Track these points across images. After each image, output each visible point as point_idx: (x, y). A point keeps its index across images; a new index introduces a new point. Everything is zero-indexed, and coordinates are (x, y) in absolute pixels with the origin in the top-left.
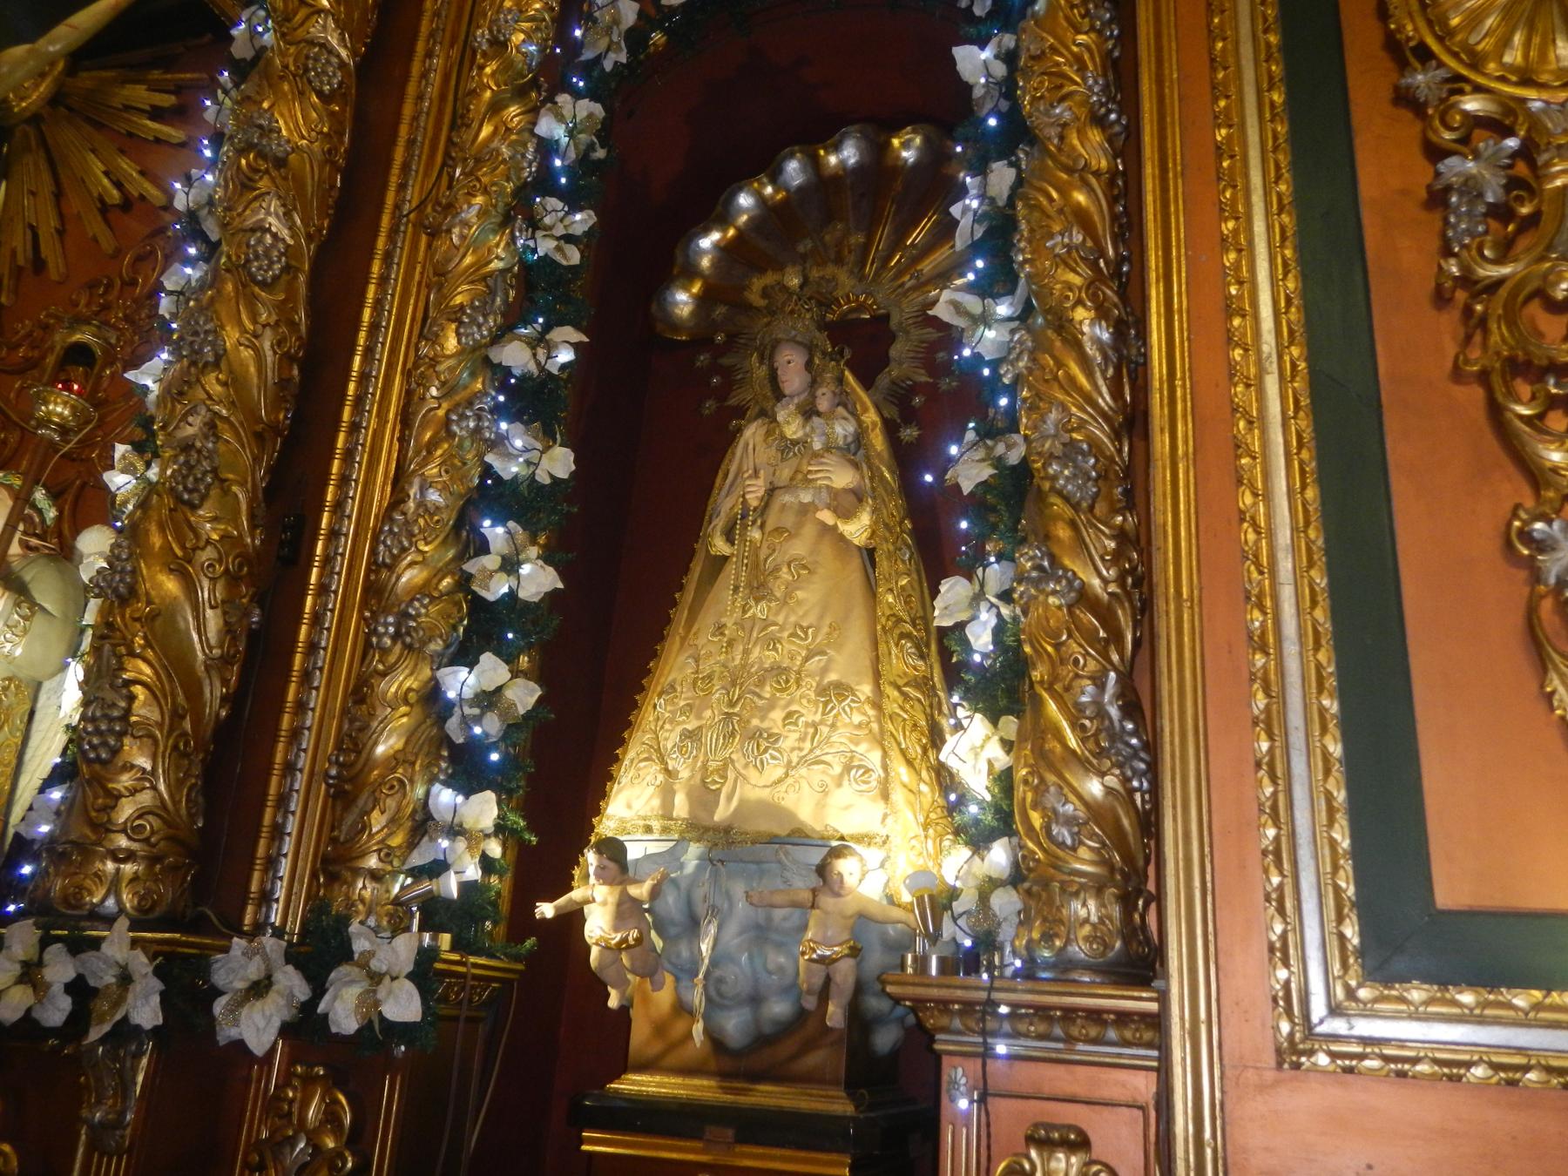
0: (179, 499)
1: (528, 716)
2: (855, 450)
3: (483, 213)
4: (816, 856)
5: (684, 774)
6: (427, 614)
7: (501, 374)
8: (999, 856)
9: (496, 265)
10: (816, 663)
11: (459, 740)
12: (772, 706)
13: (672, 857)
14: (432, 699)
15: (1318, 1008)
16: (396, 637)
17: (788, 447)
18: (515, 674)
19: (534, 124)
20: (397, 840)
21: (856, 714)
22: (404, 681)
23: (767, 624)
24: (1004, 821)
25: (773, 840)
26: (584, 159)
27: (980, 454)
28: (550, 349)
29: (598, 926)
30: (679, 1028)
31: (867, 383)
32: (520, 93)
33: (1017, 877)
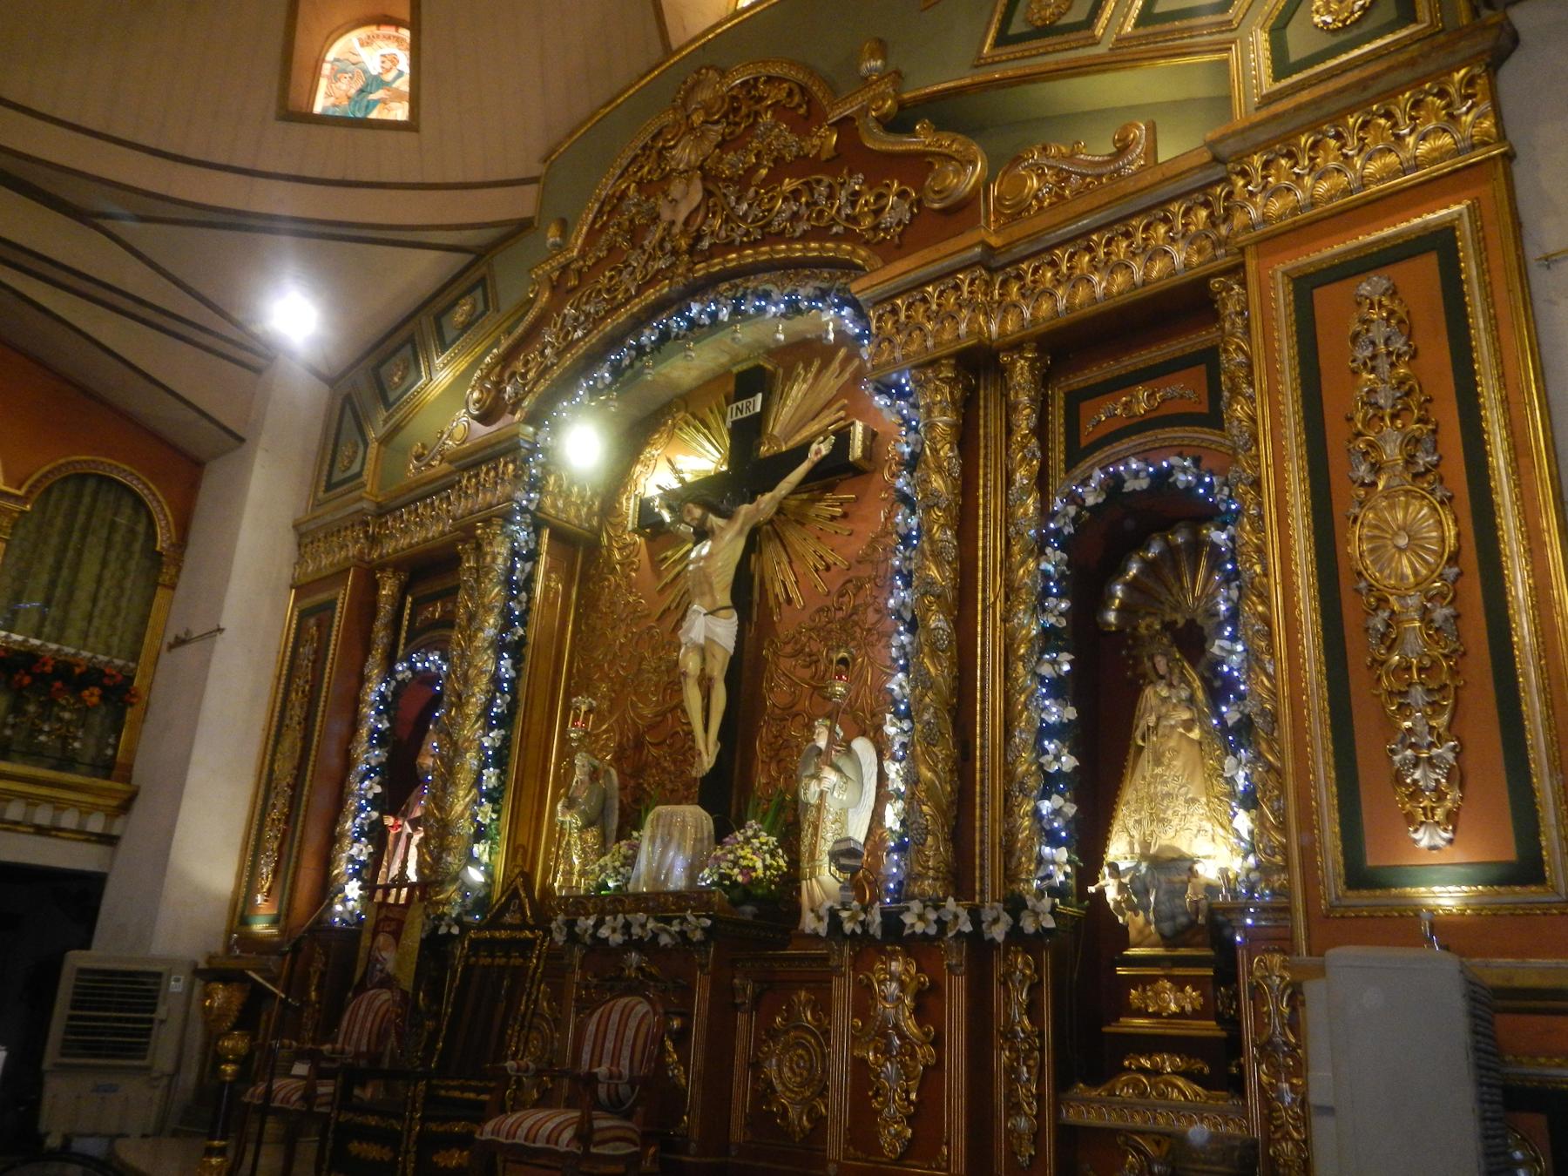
0: (928, 743)
1: (1074, 817)
2: (1191, 701)
3: (1025, 613)
4: (1188, 864)
5: (1137, 837)
6: (1031, 782)
7: (1042, 679)
9: (1034, 632)
10: (1183, 790)
11: (1048, 827)
12: (1168, 807)
13: (1136, 868)
14: (1036, 811)
16: (1020, 791)
17: (1165, 700)
18: (1066, 801)
19: (1038, 565)
20: (1032, 867)
21: (1200, 809)
22: (1027, 807)
23: (1162, 776)
24: (1253, 849)
25: (1173, 860)
26: (1063, 576)
27: (1235, 708)
28: (1059, 664)
29: (1112, 894)
30: (1147, 932)
31: (1194, 666)
32: (1031, 553)
33: (1259, 866)
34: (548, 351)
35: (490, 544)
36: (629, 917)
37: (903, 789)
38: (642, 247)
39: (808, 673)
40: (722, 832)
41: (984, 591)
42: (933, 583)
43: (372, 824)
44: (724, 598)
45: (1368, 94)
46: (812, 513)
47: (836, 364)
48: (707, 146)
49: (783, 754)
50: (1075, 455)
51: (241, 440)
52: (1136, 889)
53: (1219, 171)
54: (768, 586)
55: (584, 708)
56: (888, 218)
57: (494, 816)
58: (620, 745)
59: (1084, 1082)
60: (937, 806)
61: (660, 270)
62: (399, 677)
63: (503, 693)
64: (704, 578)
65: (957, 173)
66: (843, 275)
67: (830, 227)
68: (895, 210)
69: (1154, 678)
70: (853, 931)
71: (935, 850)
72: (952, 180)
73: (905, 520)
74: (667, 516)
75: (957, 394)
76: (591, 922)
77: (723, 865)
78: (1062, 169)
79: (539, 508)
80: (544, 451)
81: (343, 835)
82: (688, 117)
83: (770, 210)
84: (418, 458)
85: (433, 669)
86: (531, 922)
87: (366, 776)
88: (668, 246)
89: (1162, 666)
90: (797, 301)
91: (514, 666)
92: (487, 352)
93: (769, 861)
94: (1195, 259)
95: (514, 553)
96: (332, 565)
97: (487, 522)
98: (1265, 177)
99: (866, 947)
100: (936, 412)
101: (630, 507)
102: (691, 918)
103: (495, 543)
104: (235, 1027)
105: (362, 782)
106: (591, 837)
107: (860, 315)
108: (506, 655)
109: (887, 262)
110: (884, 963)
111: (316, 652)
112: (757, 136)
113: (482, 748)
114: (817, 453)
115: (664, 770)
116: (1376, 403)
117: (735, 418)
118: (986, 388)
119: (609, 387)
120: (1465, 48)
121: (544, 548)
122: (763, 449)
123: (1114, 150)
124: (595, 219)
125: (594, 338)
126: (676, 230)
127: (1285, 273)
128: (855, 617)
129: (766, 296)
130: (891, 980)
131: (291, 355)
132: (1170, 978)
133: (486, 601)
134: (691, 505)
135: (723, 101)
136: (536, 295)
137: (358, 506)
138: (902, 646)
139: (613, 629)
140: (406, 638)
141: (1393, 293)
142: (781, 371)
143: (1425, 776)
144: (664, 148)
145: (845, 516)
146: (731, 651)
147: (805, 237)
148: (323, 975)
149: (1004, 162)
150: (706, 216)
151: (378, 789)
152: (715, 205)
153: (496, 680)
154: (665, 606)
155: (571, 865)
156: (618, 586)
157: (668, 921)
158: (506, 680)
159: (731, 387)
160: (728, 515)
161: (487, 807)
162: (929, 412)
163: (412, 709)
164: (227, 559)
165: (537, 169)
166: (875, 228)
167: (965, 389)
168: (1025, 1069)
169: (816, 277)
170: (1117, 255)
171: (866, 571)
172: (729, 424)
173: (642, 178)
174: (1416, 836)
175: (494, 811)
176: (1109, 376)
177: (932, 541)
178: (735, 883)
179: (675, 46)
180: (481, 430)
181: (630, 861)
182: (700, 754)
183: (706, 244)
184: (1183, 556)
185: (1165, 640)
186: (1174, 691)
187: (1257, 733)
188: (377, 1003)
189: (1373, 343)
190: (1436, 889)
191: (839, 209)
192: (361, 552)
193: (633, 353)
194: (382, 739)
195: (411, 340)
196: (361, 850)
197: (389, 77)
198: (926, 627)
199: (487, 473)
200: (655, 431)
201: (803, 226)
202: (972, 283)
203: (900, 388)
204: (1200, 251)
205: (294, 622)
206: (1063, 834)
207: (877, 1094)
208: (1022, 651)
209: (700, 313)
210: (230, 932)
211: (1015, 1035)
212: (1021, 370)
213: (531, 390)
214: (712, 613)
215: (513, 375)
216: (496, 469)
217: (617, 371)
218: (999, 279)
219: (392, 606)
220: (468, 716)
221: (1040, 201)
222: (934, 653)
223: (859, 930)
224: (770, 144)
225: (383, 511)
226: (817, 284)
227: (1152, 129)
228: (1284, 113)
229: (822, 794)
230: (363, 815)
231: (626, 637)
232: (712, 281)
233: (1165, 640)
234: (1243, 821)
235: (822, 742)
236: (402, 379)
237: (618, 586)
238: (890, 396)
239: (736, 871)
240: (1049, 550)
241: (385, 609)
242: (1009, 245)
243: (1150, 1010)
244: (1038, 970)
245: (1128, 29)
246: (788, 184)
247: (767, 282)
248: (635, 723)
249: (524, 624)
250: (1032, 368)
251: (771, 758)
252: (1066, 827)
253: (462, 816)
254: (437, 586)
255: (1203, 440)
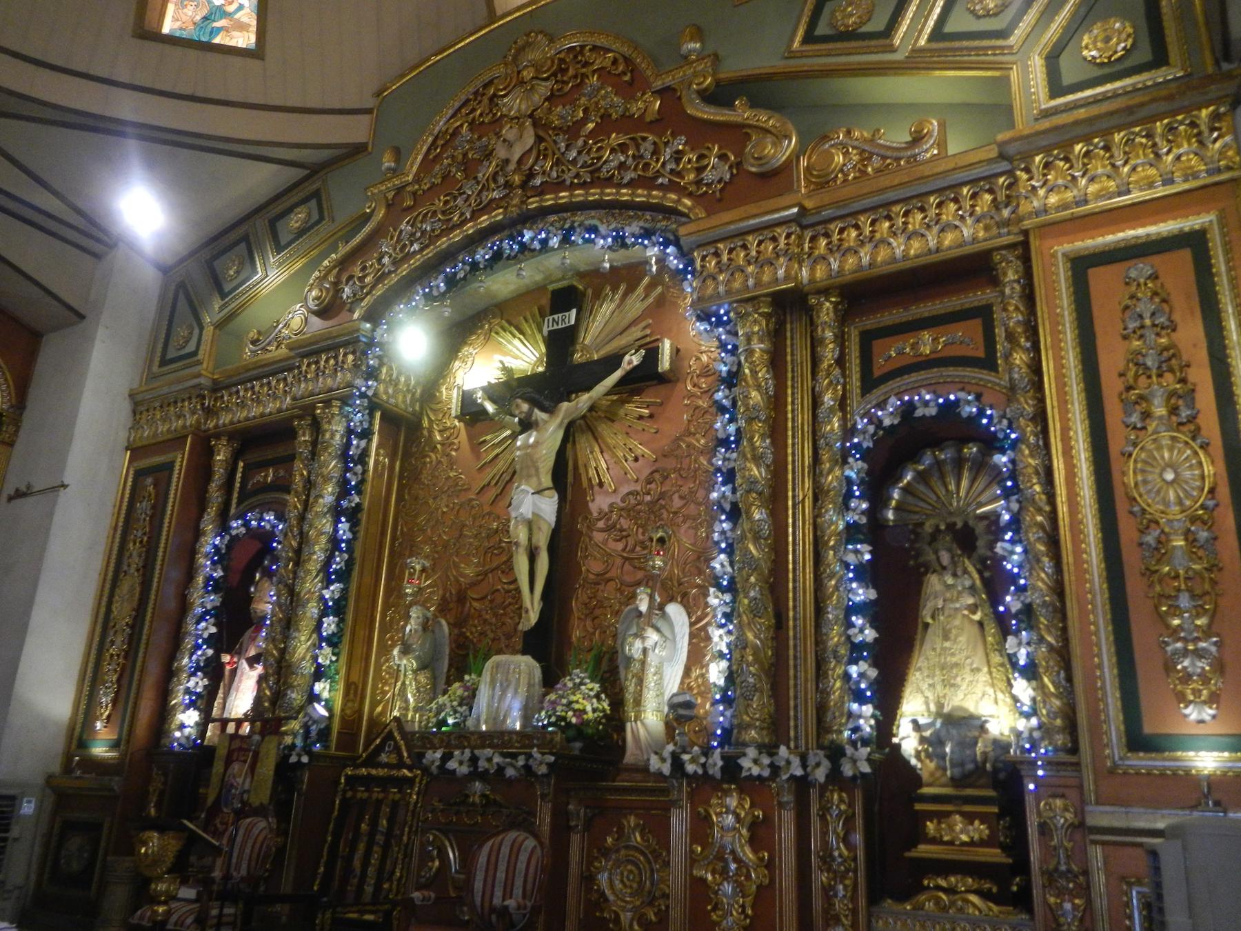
2: (972, 589)
5: (931, 698)
6: (842, 651)
8: (1034, 721)
10: (968, 661)
12: (957, 676)
14: (847, 676)
15: (1117, 758)
17: (948, 587)
21: (983, 677)
24: (1034, 712)
25: (964, 718)
28: (862, 554)
31: (969, 558)
33: (1040, 727)
34: (386, 260)
35: (329, 422)
36: (477, 752)
37: (726, 651)
38: (475, 178)
39: (620, 546)
40: (550, 681)
41: (794, 490)
42: (756, 482)
43: (207, 660)
44: (547, 481)
45: (1131, 119)
46: (622, 412)
47: (640, 290)
48: (537, 98)
49: (598, 612)
50: (869, 383)
51: (82, 317)
52: (933, 743)
53: (1005, 166)
54: (582, 470)
55: (418, 567)
56: (708, 176)
57: (334, 658)
58: (443, 598)
59: (891, 898)
60: (761, 664)
61: (492, 200)
62: (234, 532)
63: (341, 550)
64: (530, 462)
65: (774, 145)
66: (664, 218)
67: (656, 178)
68: (716, 170)
69: (938, 568)
70: (695, 772)
71: (759, 705)
72: (769, 150)
73: (724, 427)
74: (490, 408)
75: (771, 326)
76: (438, 755)
77: (559, 708)
78: (864, 151)
79: (375, 394)
80: (380, 345)
81: (180, 670)
82: (519, 72)
83: (599, 158)
84: (254, 342)
85: (268, 527)
86: (408, 761)
87: (201, 618)
88: (501, 180)
89: (945, 558)
90: (623, 237)
91: (351, 529)
92: (324, 255)
93: (596, 705)
94: (981, 234)
95: (350, 432)
96: (169, 431)
97: (327, 403)
98: (1045, 175)
99: (704, 785)
100: (755, 340)
101: (451, 397)
102: (537, 755)
103: (333, 422)
104: (169, 871)
105: (198, 623)
106: (422, 679)
107: (683, 254)
108: (343, 519)
109: (710, 213)
110: (720, 798)
111: (154, 507)
112: (584, 95)
113: (322, 598)
115: (485, 621)
116: (1144, 364)
118: (792, 323)
119: (443, 294)
120: (1214, 90)
121: (377, 427)
122: (577, 356)
123: (909, 139)
124: (429, 150)
125: (429, 252)
126: (512, 166)
127: (1064, 255)
128: (663, 502)
129: (593, 229)
130: (726, 813)
131: (132, 246)
132: (962, 814)
134: (519, 401)
135: (553, 62)
136: (373, 211)
137: (196, 381)
138: (723, 532)
139: (435, 498)
140: (239, 498)
141: (1154, 277)
142: (590, 291)
143: (1193, 664)
144: (495, 95)
145: (651, 416)
147: (631, 184)
148: (162, 793)
149: (814, 138)
150: (537, 158)
151: (213, 630)
152: (546, 149)
153: (335, 541)
154: (485, 482)
155: (407, 701)
156: (439, 462)
157: (514, 756)
158: (343, 541)
159: (545, 301)
160: (550, 410)
161: (327, 650)
162: (749, 340)
163: (241, 558)
164: (71, 424)
165: (370, 103)
166: (698, 183)
167: (776, 323)
168: (841, 887)
169: (639, 218)
170: (914, 224)
171: (671, 463)
172: (545, 332)
173: (474, 119)
174: (1187, 711)
175: (334, 654)
176: (897, 321)
177: (754, 449)
178: (569, 724)
179: (499, 12)
180: (317, 323)
181: (469, 700)
182: (527, 611)
183: (538, 181)
184: (948, 468)
185: (948, 538)
186: (959, 581)
187: (1038, 620)
188: (256, 831)
189: (1141, 316)
190: (1202, 753)
191: (664, 164)
192: (198, 421)
193: (468, 268)
194: (215, 586)
195: (245, 239)
196: (198, 683)
197: (231, 9)
198: (749, 517)
199: (327, 361)
200: (472, 333)
201: (629, 175)
202: (788, 236)
203: (719, 317)
204: (986, 228)
205: (130, 480)
206: (869, 694)
207: (715, 909)
208: (832, 543)
209: (532, 239)
210: (68, 757)
211: (834, 859)
212: (826, 310)
213: (367, 294)
214: (538, 492)
215: (351, 278)
216: (336, 358)
217: (451, 282)
218: (808, 234)
219: (226, 469)
220: (309, 572)
221: (846, 175)
222: (757, 538)
223: (700, 771)
224: (597, 103)
225: (216, 388)
226: (642, 224)
227: (942, 126)
228: (1064, 126)
229: (645, 651)
230: (200, 653)
231: (447, 506)
232: (543, 212)
233: (948, 538)
234: (1023, 689)
235: (643, 607)
236: (238, 272)
237: (439, 462)
238: (710, 324)
239: (570, 713)
240: (851, 460)
241: (219, 473)
242: (819, 209)
243: (946, 838)
244: (851, 805)
245: (922, 42)
246: (615, 139)
247: (593, 218)
248: (458, 581)
249: (359, 493)
250: (835, 308)
251: (587, 616)
252: (869, 688)
253: (303, 659)
254: (270, 454)
255: (981, 379)
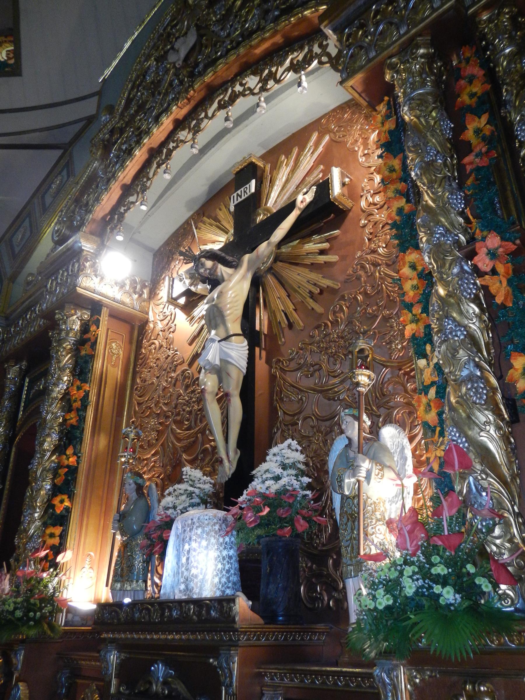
35: (65, 323)
44: (235, 327)
114: (302, 202)
117: (236, 202)
133: (62, 365)
134: (203, 260)
146: (245, 371)
160: (234, 265)
231: (167, 381)
241: (10, 388)
